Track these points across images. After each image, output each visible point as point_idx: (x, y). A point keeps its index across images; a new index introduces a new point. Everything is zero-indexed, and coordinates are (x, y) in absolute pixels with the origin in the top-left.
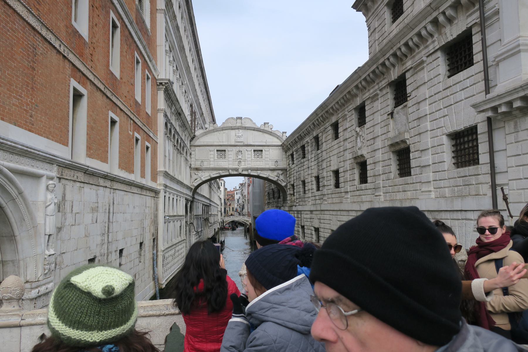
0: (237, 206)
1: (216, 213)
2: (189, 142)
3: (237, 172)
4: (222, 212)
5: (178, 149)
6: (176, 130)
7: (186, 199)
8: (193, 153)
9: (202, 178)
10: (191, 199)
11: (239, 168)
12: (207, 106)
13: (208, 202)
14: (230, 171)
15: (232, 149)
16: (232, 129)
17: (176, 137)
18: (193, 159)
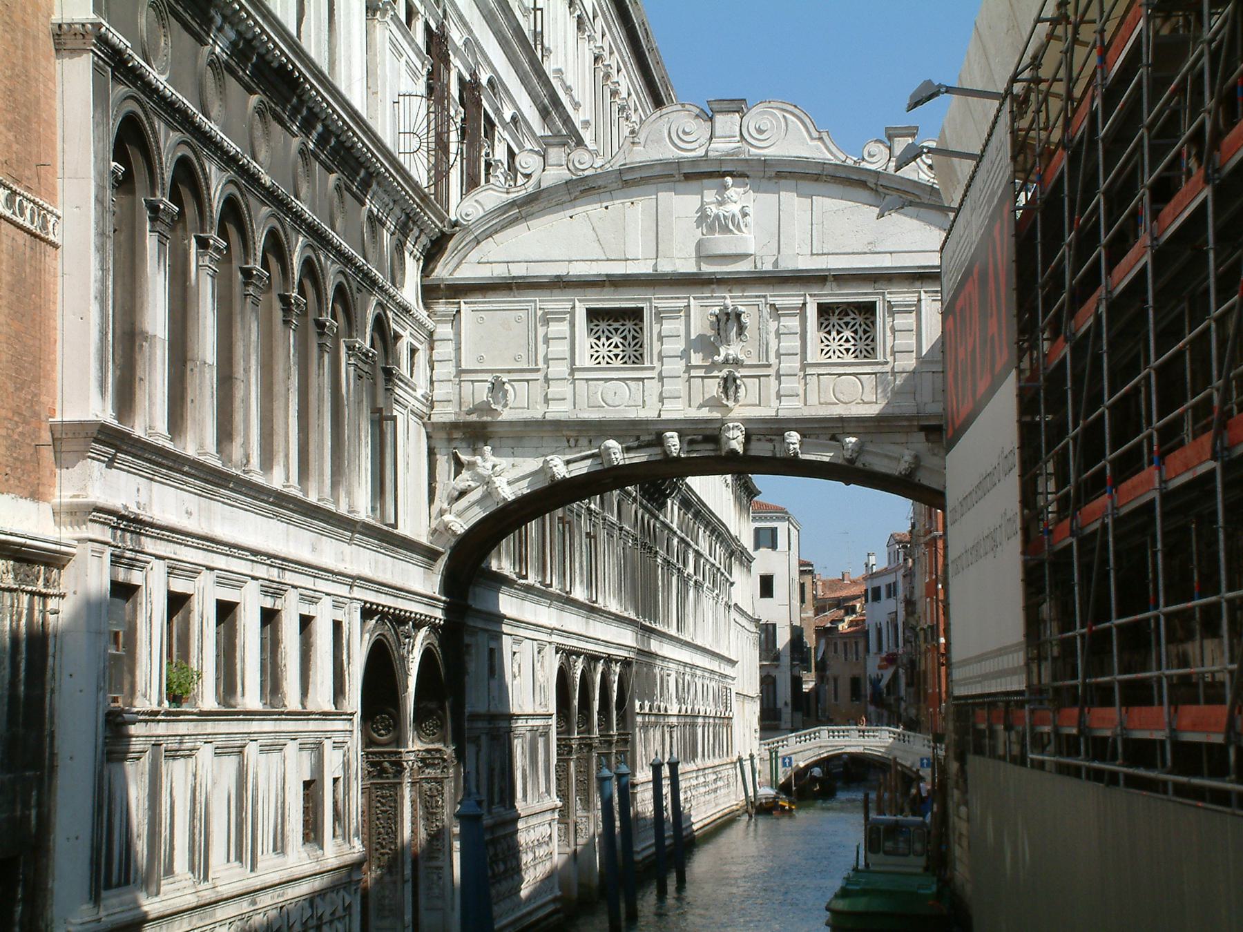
0: (880, 667)
1: (711, 710)
2: (412, 270)
3: (711, 446)
4: (780, 704)
5: (285, 299)
6: (244, 171)
7: (368, 612)
8: (444, 330)
10: (439, 614)
11: (722, 422)
12: (612, 61)
13: (628, 636)
15: (682, 303)
16: (688, 177)
17: (261, 218)
18: (442, 371)
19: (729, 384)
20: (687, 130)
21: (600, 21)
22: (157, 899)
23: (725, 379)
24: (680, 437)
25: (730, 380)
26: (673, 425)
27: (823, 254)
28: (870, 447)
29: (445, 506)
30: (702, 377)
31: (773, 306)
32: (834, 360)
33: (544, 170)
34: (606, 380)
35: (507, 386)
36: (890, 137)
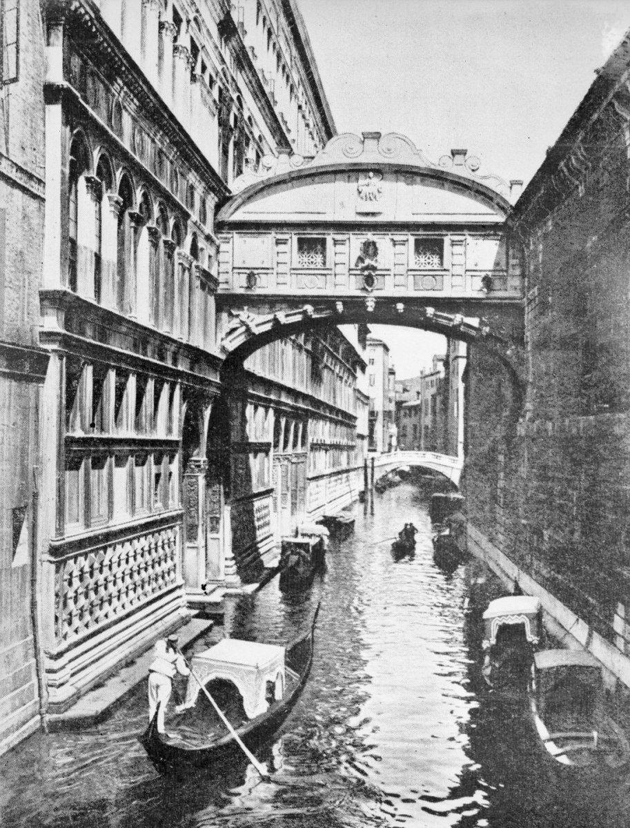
8: (223, 247)
9: (252, 325)
11: (365, 297)
19: (369, 280)
21: (301, 89)
22: (90, 529)
24: (345, 303)
26: (339, 298)
28: (439, 313)
29: (224, 336)
31: (392, 240)
32: (422, 268)
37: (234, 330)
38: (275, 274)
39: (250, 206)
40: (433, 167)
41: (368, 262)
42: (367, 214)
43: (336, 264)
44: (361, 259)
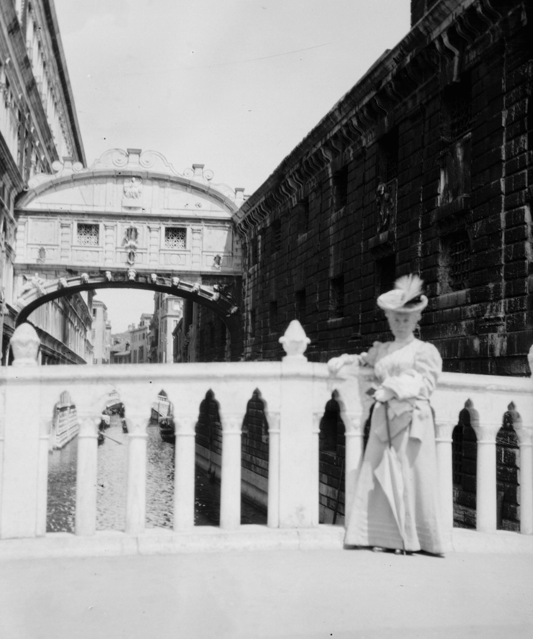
8: (20, 228)
9: (41, 287)
11: (128, 269)
14: (109, 275)
19: (131, 255)
20: (119, 159)
23: (130, 254)
24: (112, 274)
25: (132, 254)
27: (168, 209)
28: (182, 282)
29: (19, 295)
30: (121, 252)
31: (149, 227)
32: (170, 248)
33: (63, 169)
34: (84, 251)
35: (46, 251)
36: (194, 167)
37: (26, 291)
38: (60, 250)
39: (41, 199)
40: (180, 176)
41: (131, 242)
42: (130, 208)
43: (106, 244)
44: (125, 241)
